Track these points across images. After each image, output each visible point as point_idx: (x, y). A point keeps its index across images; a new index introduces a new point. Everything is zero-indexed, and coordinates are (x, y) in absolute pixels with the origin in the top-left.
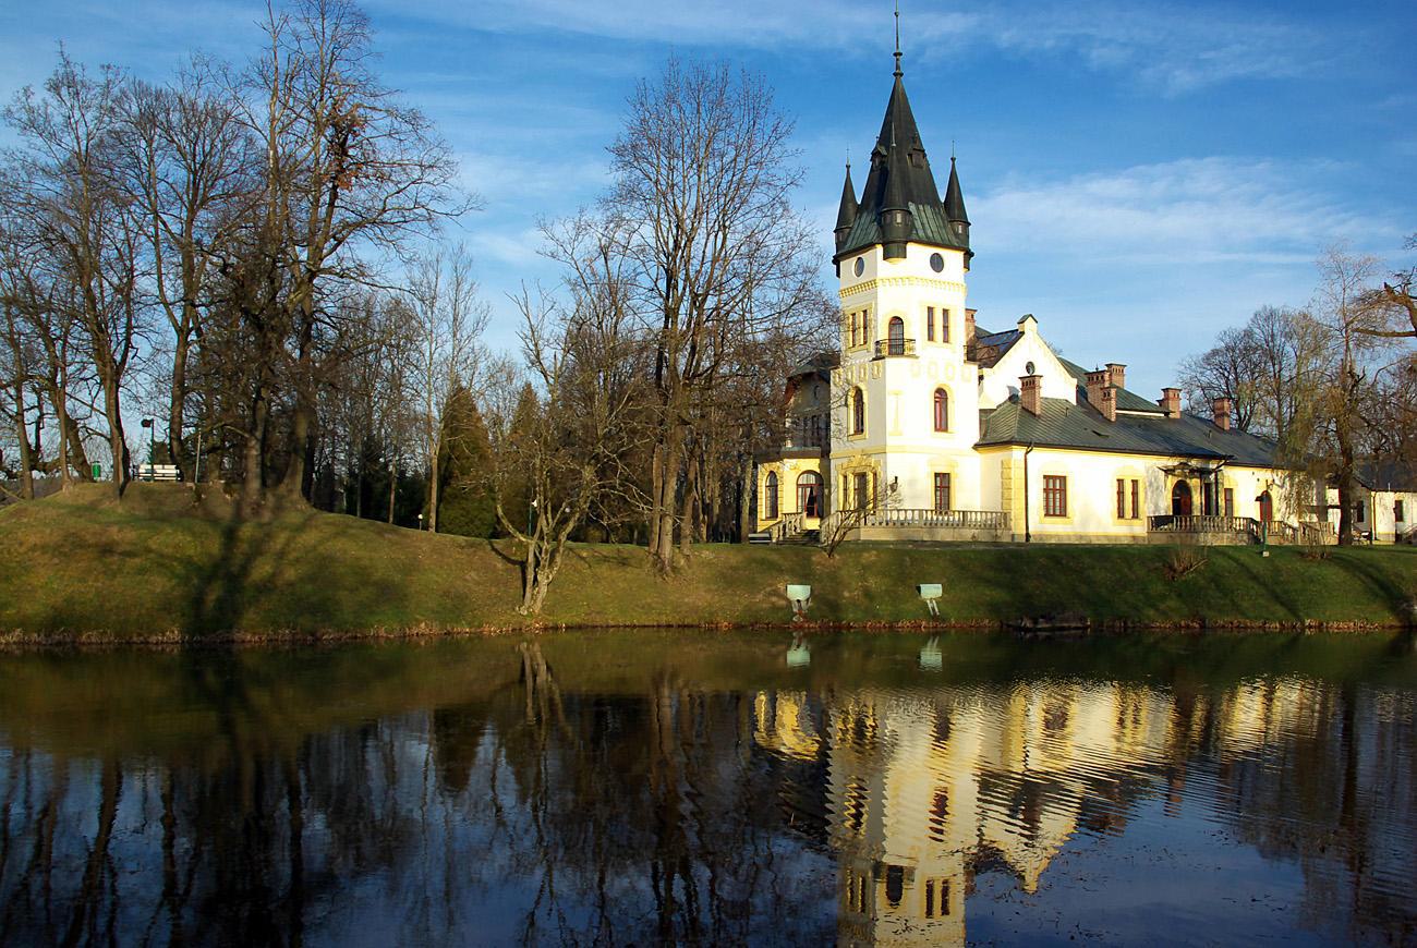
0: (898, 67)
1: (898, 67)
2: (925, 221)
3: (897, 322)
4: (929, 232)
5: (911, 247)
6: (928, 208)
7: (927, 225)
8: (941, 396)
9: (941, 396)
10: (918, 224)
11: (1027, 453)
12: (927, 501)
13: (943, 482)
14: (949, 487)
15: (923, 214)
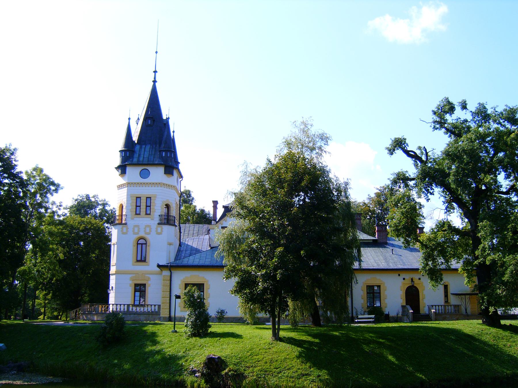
0: (155, 78)
1: (155, 78)
2: (142, 153)
3: (122, 207)
4: (141, 159)
5: (129, 169)
6: (148, 147)
7: (142, 156)
8: (142, 244)
9: (142, 244)
10: (136, 156)
11: (171, 272)
12: (128, 298)
13: (140, 289)
14: (145, 291)
15: (143, 150)
